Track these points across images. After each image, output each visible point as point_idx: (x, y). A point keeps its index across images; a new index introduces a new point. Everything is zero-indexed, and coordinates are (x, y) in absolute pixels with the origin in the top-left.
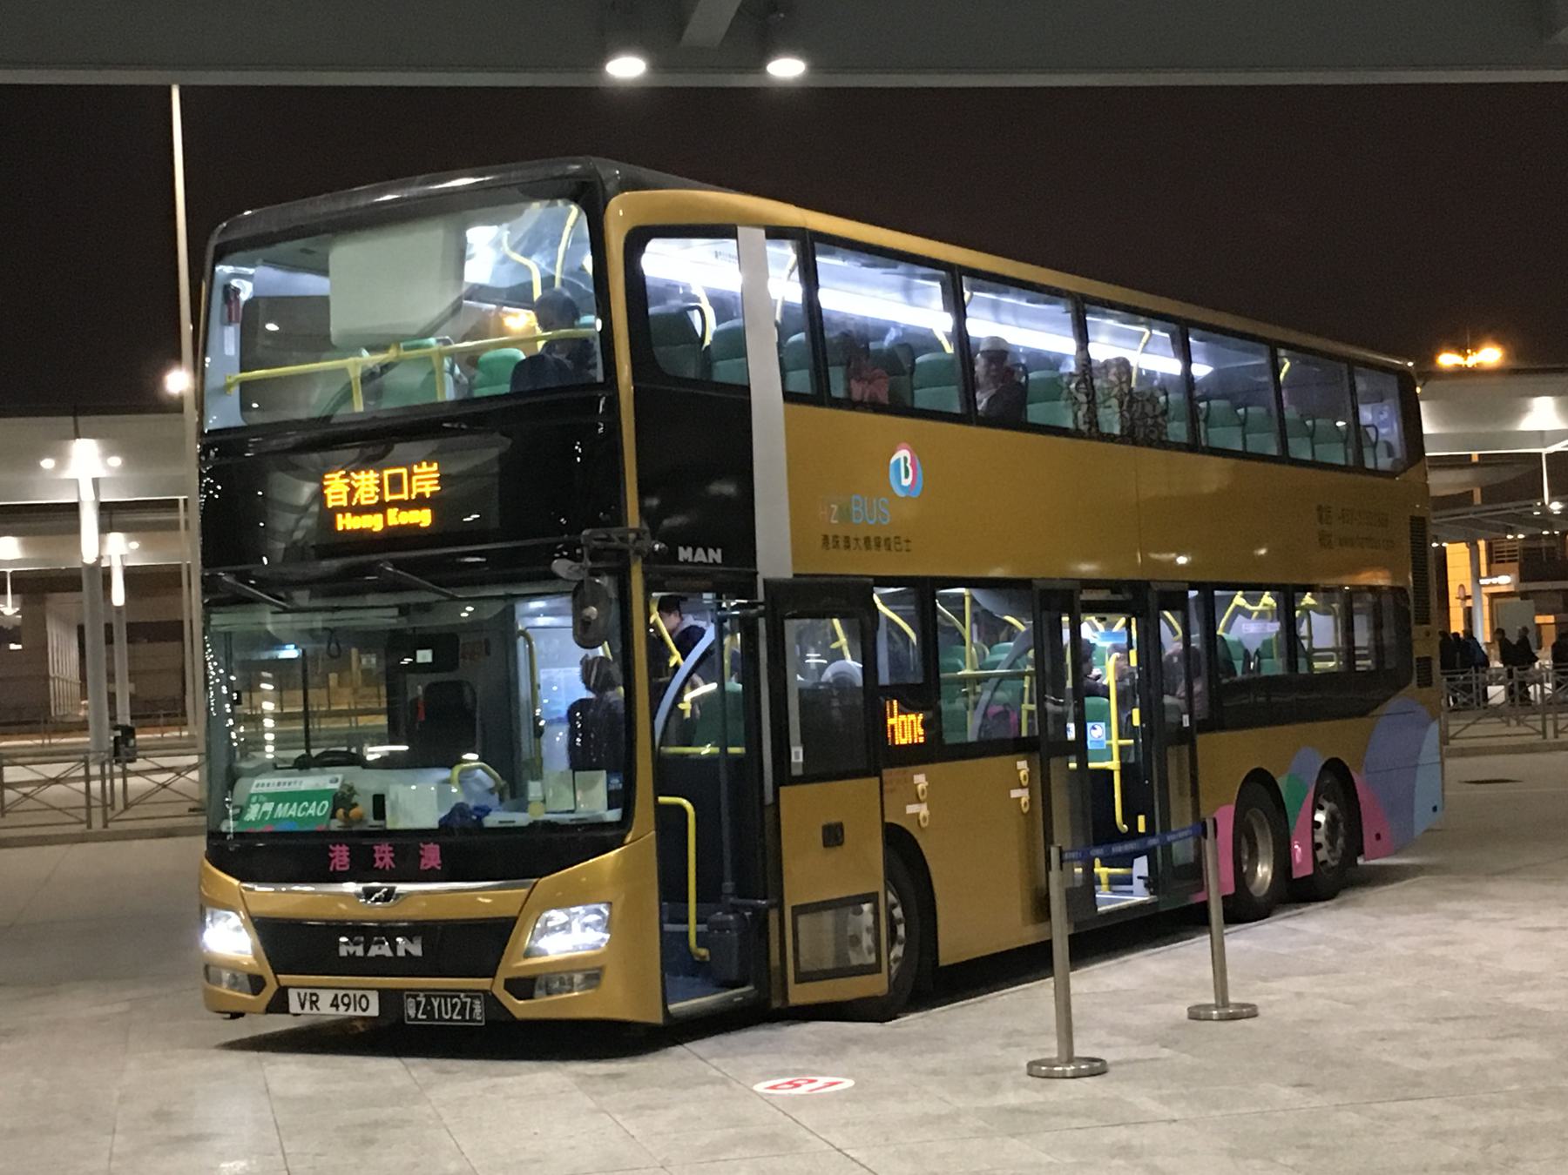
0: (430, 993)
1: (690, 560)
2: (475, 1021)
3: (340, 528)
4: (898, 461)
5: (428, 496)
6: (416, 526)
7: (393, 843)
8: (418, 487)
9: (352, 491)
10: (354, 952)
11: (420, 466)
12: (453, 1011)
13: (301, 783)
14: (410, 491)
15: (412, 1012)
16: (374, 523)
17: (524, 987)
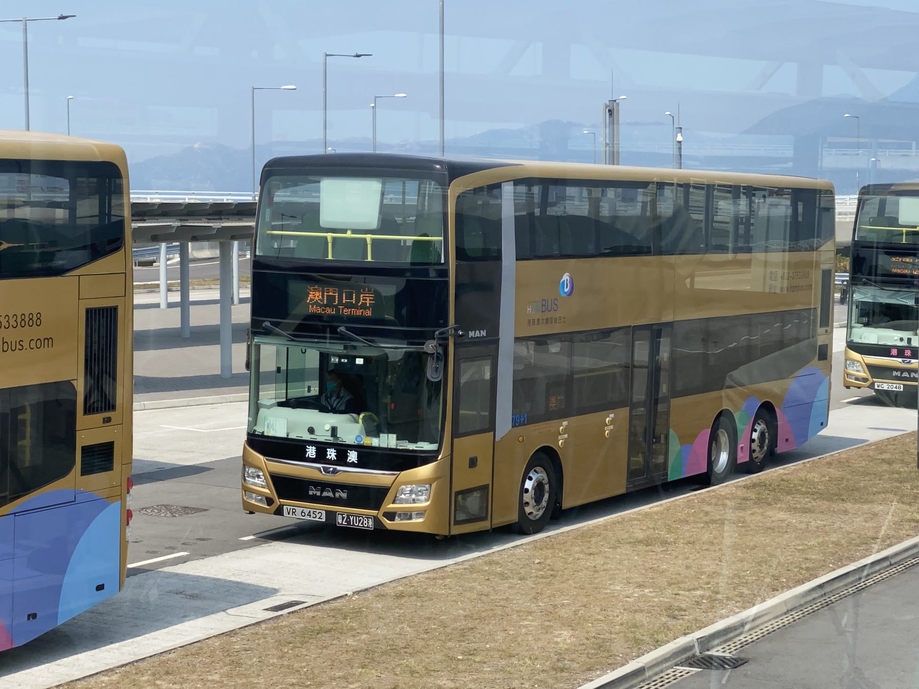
2: (369, 528)
15: (340, 521)
17: (391, 516)
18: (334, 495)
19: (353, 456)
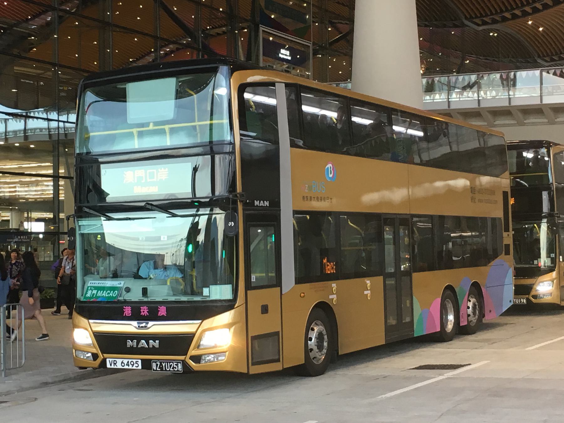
1: (259, 205)
2: (179, 371)
4: (328, 168)
7: (149, 306)
10: (133, 346)
12: (170, 367)
13: (107, 283)
17: (197, 359)
19: (163, 311)
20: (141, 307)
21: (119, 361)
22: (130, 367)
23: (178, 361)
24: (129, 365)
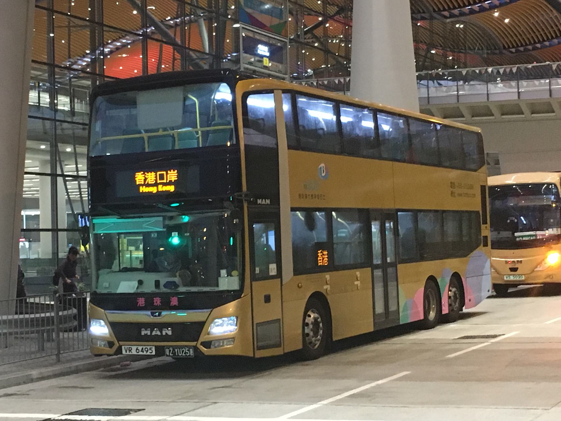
0: (174, 347)
2: (191, 356)
3: (141, 191)
4: (321, 168)
5: (173, 181)
6: (169, 191)
8: (170, 178)
9: (145, 179)
11: (170, 171)
12: (182, 352)
14: (167, 180)
16: (154, 190)
17: (207, 344)
18: (161, 332)
20: (154, 298)
21: (134, 348)
22: (145, 353)
23: (189, 347)
24: (143, 352)
